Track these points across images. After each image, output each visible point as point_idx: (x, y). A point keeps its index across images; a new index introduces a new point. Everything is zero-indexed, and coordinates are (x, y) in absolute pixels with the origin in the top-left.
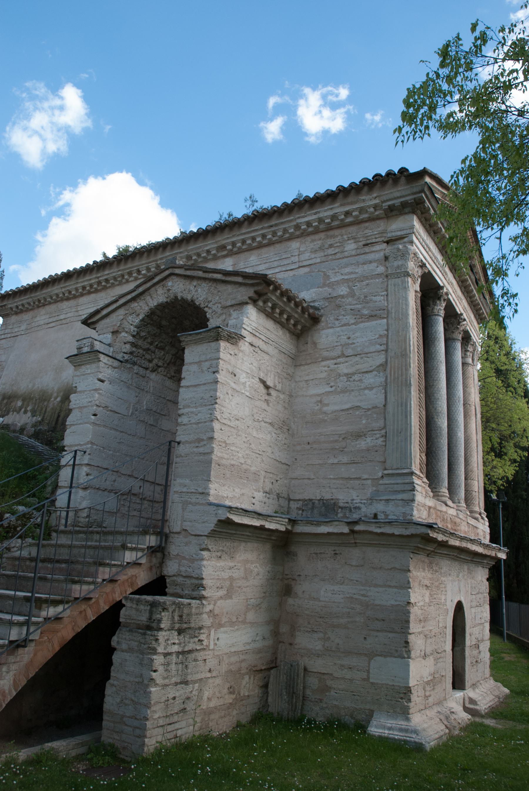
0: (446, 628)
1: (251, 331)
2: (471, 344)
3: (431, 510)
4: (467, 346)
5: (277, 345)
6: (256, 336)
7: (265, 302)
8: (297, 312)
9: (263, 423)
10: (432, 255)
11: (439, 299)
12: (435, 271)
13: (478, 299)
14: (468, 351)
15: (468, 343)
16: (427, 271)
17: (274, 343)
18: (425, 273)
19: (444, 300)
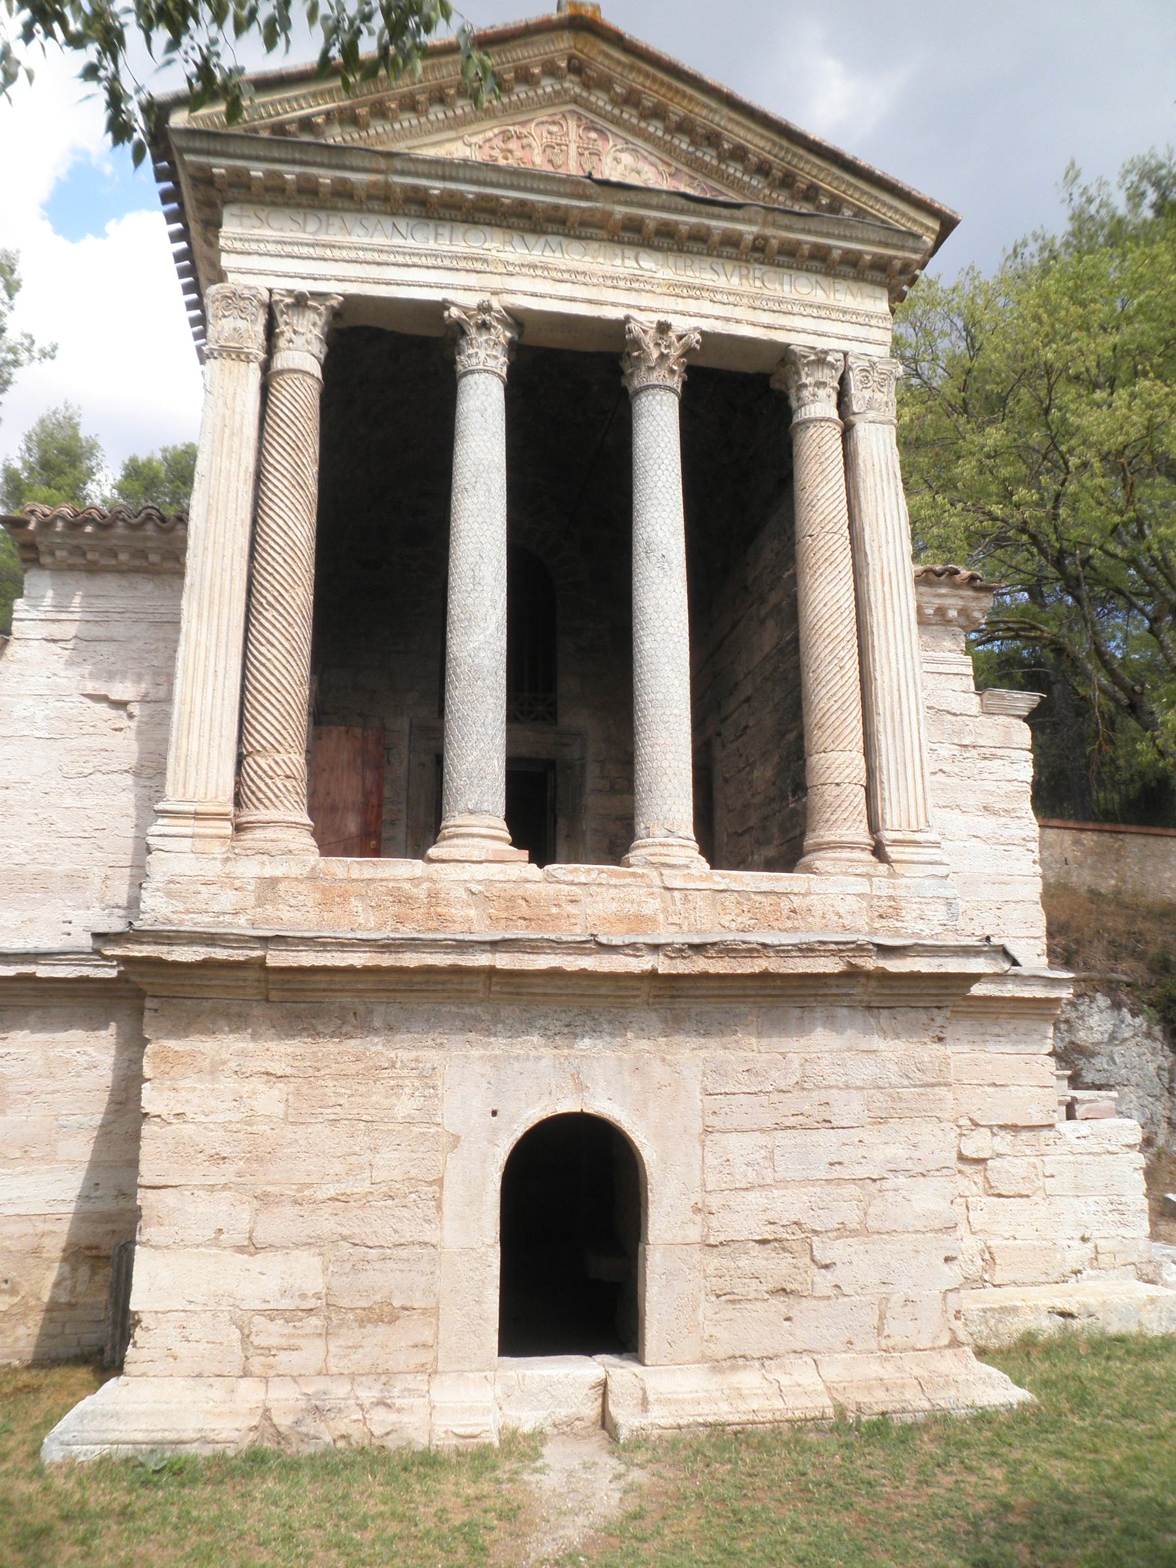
0: (440, 1182)
1: (43, 617)
2: (809, 364)
3: (282, 887)
4: (798, 373)
5: (138, 616)
6: (59, 621)
7: (52, 553)
8: (145, 538)
9: (99, 775)
10: (353, 255)
11: (458, 331)
13: (769, 232)
14: (805, 386)
15: (794, 364)
16: (334, 303)
17: (128, 615)
18: (332, 307)
19: (484, 326)
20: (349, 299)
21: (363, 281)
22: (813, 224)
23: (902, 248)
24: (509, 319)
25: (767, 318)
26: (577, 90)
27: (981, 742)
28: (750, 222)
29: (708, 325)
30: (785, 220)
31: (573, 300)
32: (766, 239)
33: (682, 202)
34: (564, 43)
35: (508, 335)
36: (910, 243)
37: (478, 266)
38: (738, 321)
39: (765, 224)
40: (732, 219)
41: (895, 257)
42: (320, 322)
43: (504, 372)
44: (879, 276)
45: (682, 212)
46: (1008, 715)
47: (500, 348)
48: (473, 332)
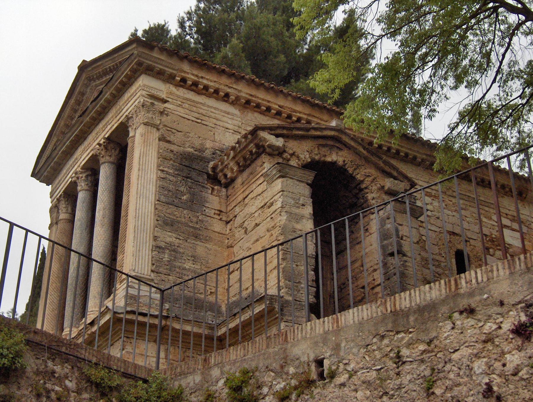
12: (67, 182)
16: (62, 196)
19: (78, 178)
20: (64, 192)
21: (65, 185)
22: (115, 78)
23: (133, 61)
24: (83, 171)
25: (118, 118)
26: (94, 84)
27: (267, 200)
28: (107, 92)
29: (106, 136)
30: (110, 84)
31: (89, 154)
32: (112, 93)
33: (94, 103)
34: (84, 76)
35: (84, 175)
36: (133, 58)
37: (76, 161)
38: (113, 125)
39: (109, 89)
40: (104, 96)
41: (133, 66)
42: (63, 202)
43: (86, 187)
44: (138, 73)
45: (96, 105)
46: (275, 180)
47: (83, 181)
48: (77, 181)
